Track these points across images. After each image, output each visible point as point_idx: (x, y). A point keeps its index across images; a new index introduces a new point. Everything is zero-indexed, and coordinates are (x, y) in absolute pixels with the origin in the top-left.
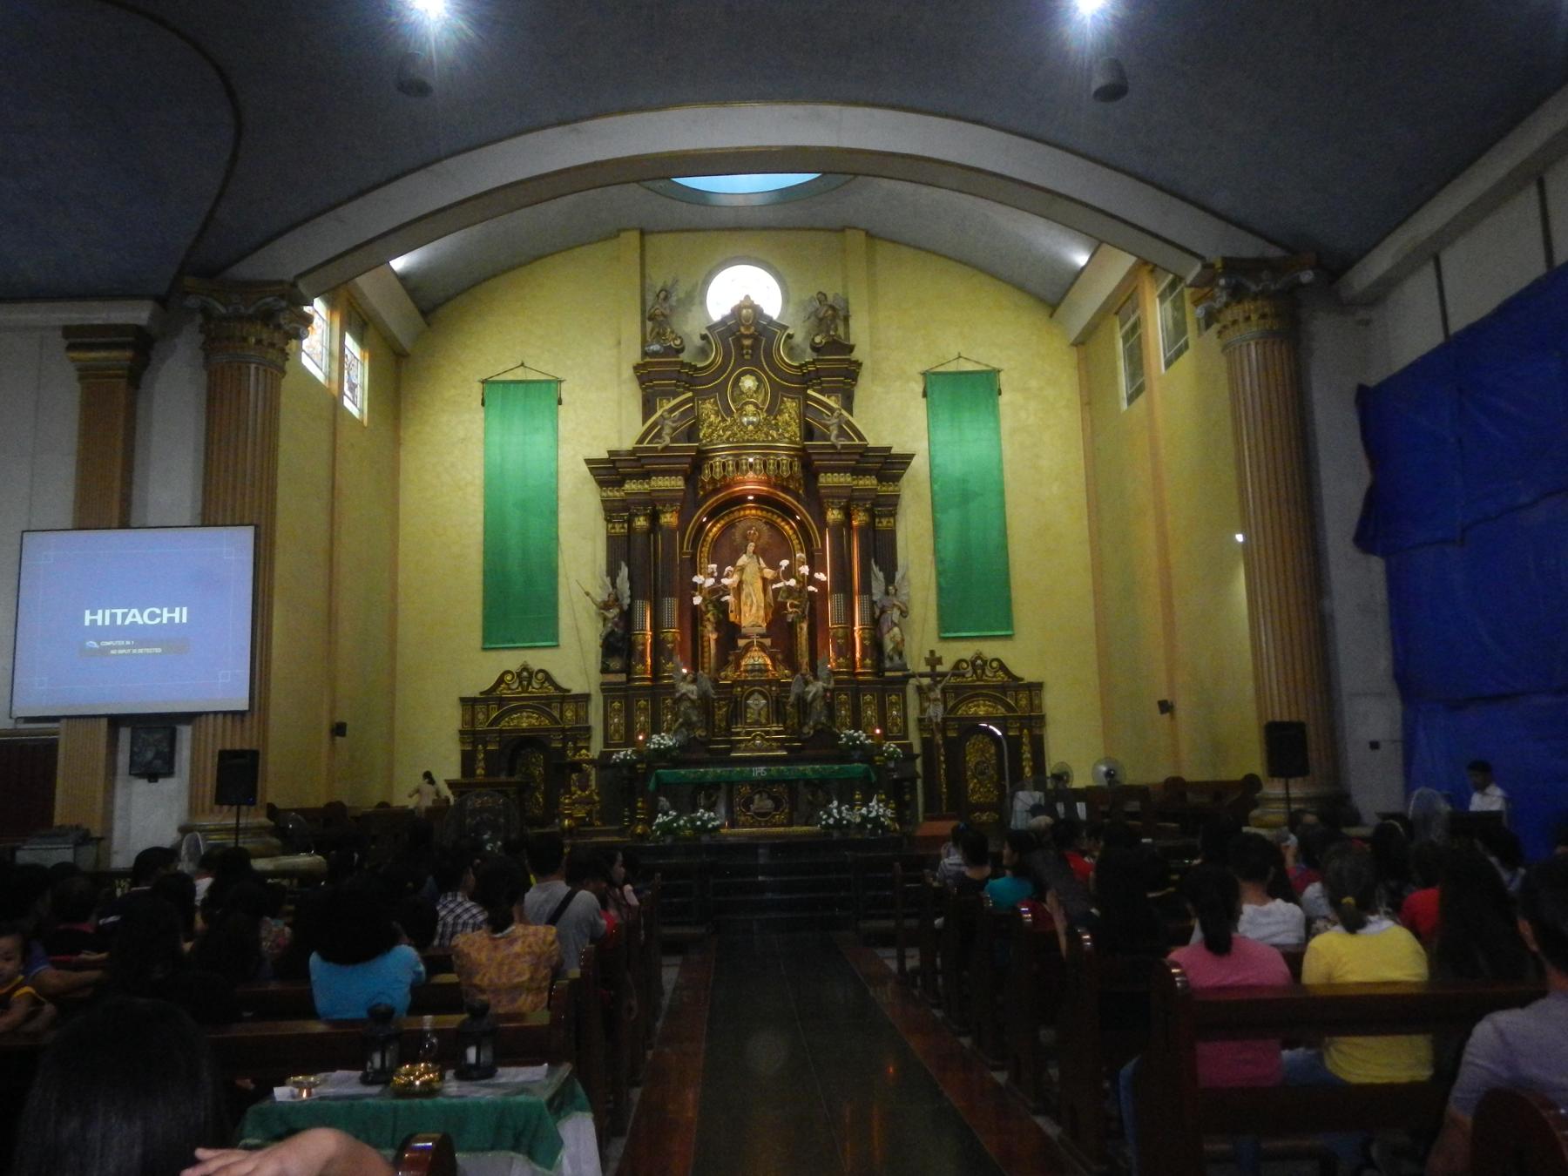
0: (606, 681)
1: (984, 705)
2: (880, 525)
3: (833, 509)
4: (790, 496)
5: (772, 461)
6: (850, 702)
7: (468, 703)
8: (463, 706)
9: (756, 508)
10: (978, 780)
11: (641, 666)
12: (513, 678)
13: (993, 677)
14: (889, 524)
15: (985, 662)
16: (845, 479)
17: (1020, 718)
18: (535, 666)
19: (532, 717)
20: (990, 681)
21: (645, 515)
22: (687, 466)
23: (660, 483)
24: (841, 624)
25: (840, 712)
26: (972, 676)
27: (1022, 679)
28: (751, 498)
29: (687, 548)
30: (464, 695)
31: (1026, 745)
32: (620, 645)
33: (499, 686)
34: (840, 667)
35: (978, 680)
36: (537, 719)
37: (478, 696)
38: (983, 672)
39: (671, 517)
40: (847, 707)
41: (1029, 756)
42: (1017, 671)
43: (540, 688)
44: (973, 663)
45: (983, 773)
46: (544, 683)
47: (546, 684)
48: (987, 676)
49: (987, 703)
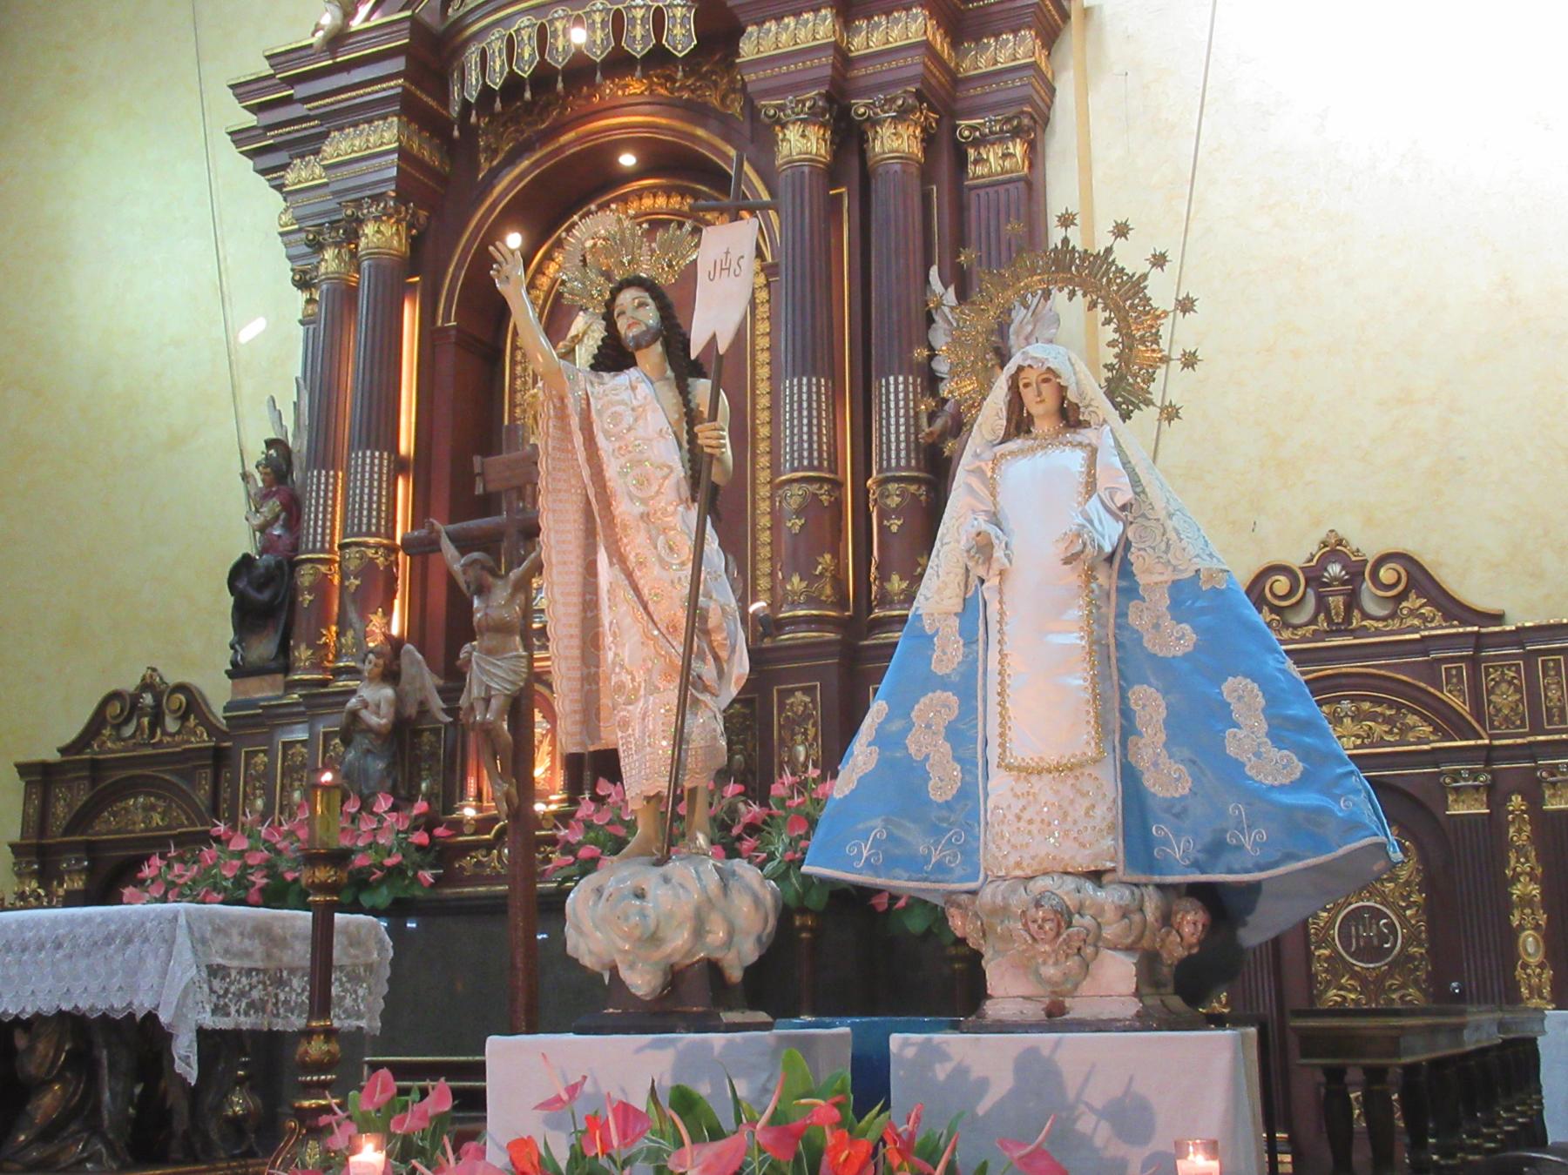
0: (240, 698)
1: (1358, 717)
2: (980, 170)
3: (784, 126)
4: (704, 126)
5: (598, 18)
6: (817, 713)
7: (39, 776)
8: (28, 783)
9: (653, 191)
10: (1354, 975)
11: (303, 647)
12: (122, 710)
13: (1393, 616)
14: (1007, 164)
15: (1355, 572)
16: (818, 27)
17: (1489, 755)
18: (173, 679)
19: (153, 808)
20: (1378, 632)
21: (337, 245)
22: (401, 81)
23: (344, 146)
24: (805, 469)
25: (791, 750)
26: (1313, 621)
27: (1498, 618)
28: (628, 160)
29: (447, 318)
30: (22, 759)
31: (1520, 850)
32: (265, 596)
33: (98, 733)
34: (794, 605)
35: (1339, 632)
36: (164, 815)
37: (54, 757)
38: (1352, 601)
39: (379, 231)
40: (811, 732)
41: (1535, 890)
42: (1474, 591)
43: (179, 732)
44: (1314, 576)
45: (1372, 951)
46: (184, 718)
47: (192, 721)
48: (1366, 616)
49: (1366, 706)
